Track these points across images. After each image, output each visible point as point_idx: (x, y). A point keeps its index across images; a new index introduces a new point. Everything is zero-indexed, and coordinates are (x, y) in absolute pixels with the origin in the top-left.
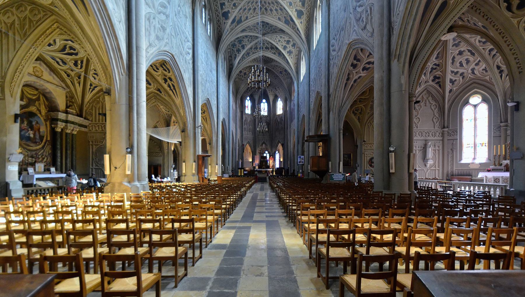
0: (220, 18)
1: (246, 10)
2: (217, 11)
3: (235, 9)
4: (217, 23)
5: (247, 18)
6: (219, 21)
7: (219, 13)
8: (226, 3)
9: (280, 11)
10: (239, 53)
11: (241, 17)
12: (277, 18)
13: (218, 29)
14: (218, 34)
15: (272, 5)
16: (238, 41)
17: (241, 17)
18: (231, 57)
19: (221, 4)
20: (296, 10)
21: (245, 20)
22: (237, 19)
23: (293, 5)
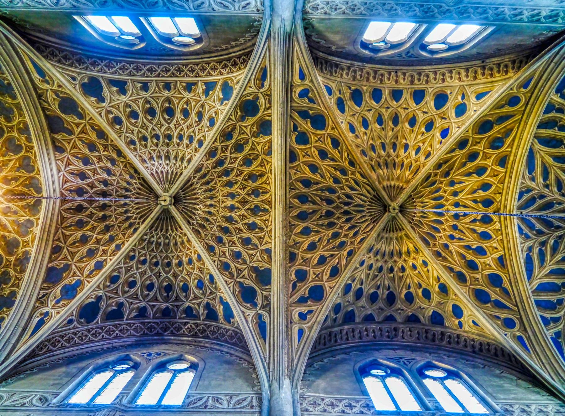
0: (86, 69)
1: (87, 151)
2: (108, 66)
3: (107, 118)
6: (79, 61)
7: (101, 71)
9: (84, 250)
11: (71, 132)
12: (57, 243)
13: (61, 50)
14: (47, 47)
15: (102, 226)
17: (71, 132)
19: (125, 83)
20: (99, 298)
21: (53, 141)
23: (113, 286)
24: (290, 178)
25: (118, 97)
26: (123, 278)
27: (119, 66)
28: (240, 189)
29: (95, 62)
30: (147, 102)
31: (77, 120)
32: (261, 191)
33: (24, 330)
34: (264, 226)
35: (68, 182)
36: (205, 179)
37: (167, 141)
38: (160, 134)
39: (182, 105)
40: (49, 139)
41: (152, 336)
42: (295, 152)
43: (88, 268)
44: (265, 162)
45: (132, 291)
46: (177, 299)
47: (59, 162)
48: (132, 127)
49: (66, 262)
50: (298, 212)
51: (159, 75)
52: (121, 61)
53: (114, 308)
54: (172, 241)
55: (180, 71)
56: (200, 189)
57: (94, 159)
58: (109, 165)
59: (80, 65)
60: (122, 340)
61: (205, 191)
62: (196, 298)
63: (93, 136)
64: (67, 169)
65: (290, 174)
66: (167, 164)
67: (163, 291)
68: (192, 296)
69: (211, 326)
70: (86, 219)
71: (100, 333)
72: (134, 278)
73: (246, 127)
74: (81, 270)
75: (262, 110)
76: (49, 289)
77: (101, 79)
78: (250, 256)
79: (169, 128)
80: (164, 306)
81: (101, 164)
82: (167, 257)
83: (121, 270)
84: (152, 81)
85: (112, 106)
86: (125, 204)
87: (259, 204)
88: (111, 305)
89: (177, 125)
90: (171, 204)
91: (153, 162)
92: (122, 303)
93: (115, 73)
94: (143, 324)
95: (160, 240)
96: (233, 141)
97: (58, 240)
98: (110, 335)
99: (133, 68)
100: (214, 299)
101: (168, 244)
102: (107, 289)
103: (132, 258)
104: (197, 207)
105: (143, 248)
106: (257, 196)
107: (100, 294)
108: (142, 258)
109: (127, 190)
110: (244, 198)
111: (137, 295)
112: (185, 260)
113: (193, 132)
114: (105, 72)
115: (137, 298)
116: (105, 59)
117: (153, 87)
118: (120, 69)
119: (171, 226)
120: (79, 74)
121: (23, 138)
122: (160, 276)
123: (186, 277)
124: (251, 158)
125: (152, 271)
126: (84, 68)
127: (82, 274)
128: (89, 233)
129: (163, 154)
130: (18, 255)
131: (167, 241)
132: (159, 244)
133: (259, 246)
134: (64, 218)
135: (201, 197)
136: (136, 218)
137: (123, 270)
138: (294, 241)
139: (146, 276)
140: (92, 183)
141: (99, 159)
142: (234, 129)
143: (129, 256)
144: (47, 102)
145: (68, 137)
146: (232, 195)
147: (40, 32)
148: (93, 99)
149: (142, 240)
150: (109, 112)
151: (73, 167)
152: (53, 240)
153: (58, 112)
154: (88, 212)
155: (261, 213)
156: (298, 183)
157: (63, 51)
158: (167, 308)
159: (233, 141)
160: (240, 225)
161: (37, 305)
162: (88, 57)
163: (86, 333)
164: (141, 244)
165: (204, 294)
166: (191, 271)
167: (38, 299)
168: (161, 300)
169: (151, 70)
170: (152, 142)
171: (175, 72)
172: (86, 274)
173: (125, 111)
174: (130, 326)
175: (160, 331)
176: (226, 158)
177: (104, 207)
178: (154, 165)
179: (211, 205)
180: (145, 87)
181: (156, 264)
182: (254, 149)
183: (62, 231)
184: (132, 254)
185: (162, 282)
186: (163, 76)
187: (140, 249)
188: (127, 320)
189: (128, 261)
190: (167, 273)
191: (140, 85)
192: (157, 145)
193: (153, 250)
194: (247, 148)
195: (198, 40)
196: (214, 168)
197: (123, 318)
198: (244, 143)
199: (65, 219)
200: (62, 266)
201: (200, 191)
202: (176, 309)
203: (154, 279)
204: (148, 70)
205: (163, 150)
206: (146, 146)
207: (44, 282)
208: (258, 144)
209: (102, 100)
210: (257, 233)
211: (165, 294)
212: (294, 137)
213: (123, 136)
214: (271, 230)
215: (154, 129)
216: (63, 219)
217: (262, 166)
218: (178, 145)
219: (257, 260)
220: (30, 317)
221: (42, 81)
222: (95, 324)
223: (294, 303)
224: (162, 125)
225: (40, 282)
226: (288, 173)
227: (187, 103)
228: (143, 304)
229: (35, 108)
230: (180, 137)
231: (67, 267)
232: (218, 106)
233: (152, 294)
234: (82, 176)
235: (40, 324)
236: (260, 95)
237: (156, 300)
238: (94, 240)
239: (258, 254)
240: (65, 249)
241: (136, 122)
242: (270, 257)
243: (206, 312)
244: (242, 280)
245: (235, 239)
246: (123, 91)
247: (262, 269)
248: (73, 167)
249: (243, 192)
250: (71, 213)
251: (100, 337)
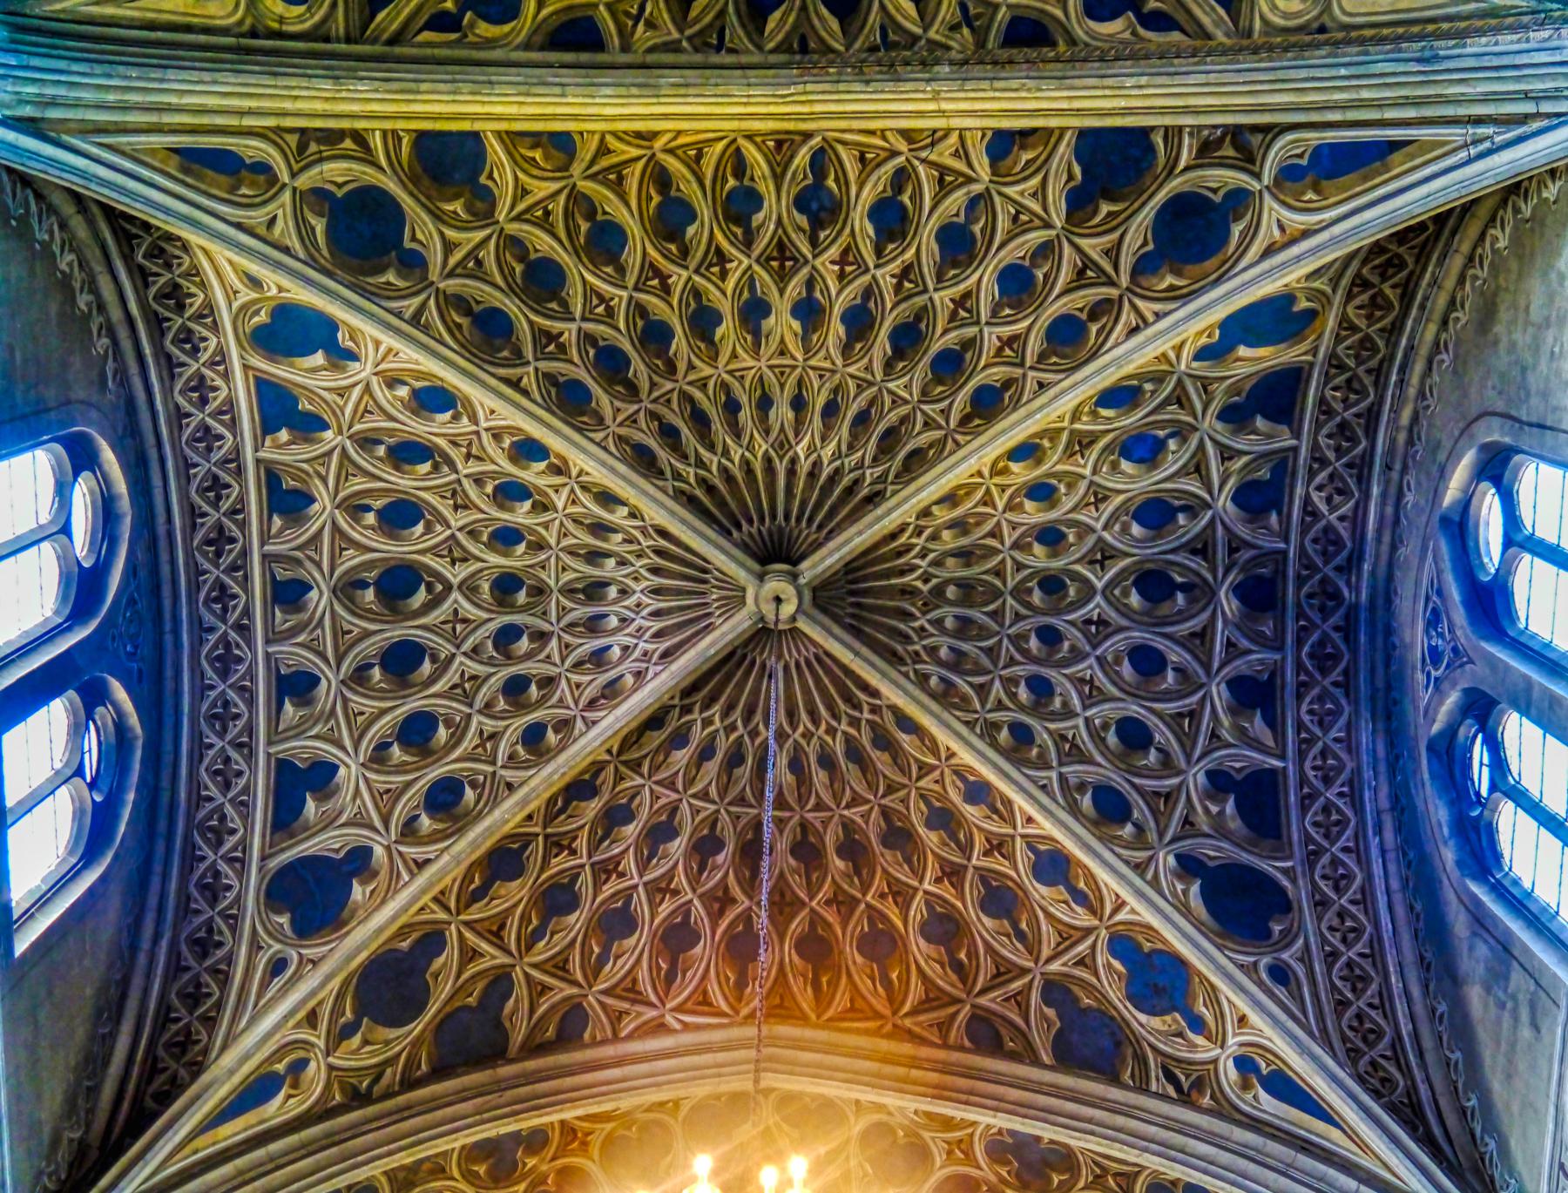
0: (234, 921)
1: (576, 920)
3: (434, 838)
4: (176, 968)
6: (204, 945)
7: (240, 863)
8: (349, 773)
9: (985, 926)
11: (500, 983)
13: (165, 1016)
14: (152, 1068)
15: (888, 860)
17: (500, 983)
19: (283, 768)
20: (1189, 866)
23: (1140, 810)
24: (672, 47)
25: (346, 795)
26: (1105, 771)
27: (214, 791)
28: (724, 275)
29: (203, 887)
30: (359, 676)
31: (449, 957)
32: (732, 182)
33: (1305, 1146)
34: (889, 167)
35: (705, 993)
36: (685, 431)
37: (522, 597)
38: (493, 626)
39: (365, 532)
40: (531, 1064)
41: (1354, 651)
42: (555, 22)
43: (1059, 912)
44: (605, 162)
45: (1162, 734)
46: (1201, 548)
47: (628, 1026)
48: (469, 741)
49: (1035, 997)
50: (824, 11)
51: (244, 629)
52: (195, 784)
53: (1230, 807)
54: (953, 569)
55: (220, 539)
56: (726, 453)
57: (608, 889)
58: (631, 830)
59: (220, 944)
60: (1367, 774)
61: (737, 433)
62: (1198, 468)
63: (514, 894)
64: (653, 998)
65: (651, 50)
66: (624, 592)
67: (1165, 609)
68: (1192, 486)
69: (1322, 401)
70: (860, 922)
71: (1335, 862)
72: (1105, 726)
73: (449, 246)
74: (1069, 936)
75: (370, 176)
76: (1141, 1060)
77: (274, 863)
78: (1019, 226)
79: (469, 588)
80: (1229, 604)
81: (630, 863)
82: (1020, 592)
83: (1073, 780)
84: (268, 656)
85: (386, 822)
86: (796, 765)
87: (790, 191)
88: (1218, 821)
89: (453, 552)
90: (794, 577)
91: (616, 652)
92: (1210, 774)
93: (244, 808)
94: (1302, 689)
95: (949, 623)
96: (512, 307)
97: (943, 1027)
98: (1342, 823)
99: (221, 734)
100: (1205, 384)
101: (965, 586)
102: (1152, 836)
103: (1022, 734)
104: (804, 467)
105: (982, 690)
106: (755, 200)
107: (1171, 860)
108: (1023, 694)
109: (735, 758)
110: (764, 261)
111: (1181, 715)
112: (1033, 514)
113: (478, 481)
114: (244, 845)
115: (1194, 715)
117: (294, 655)
118: (227, 786)
119: (887, 574)
120: (256, 946)
121: (531, 1162)
122: (1102, 622)
123: (1109, 508)
124: (584, 226)
125: (1077, 656)
126: (233, 929)
127: (1088, 931)
128: (917, 908)
129: (581, 612)
130: (1003, 1181)
131: (951, 592)
132: (965, 627)
133: (977, 188)
134: (852, 1009)
135: (762, 446)
136: (855, 723)
137: (1073, 771)
138: (954, 28)
139: (1101, 678)
140: (706, 898)
141: (606, 870)
142: (460, 303)
143: (1015, 750)
144: (378, 1071)
145: (521, 990)
146: (754, 312)
147: (94, 1091)
148: (358, 892)
149: (945, 694)
150: (409, 830)
151: (643, 974)
152: (945, 1046)
153: (417, 1027)
154: (830, 916)
155: (831, 183)
156: (693, 14)
157: (165, 1010)
158: (1239, 590)
159: (512, 307)
160: (885, 277)
161: (1206, 1101)
162: (185, 910)
163: (1330, 917)
164: (965, 699)
165: (1182, 432)
166: (1082, 487)
167: (1185, 1098)
168: (1205, 616)
169: (225, 662)
170: (529, 656)
171: (225, 561)
172: (1083, 918)
173: (401, 768)
174: (1310, 742)
175: (1336, 619)
176: (588, 339)
177: (807, 851)
178: (625, 649)
179: (798, 404)
180: (297, 686)
181: (1050, 637)
182: (547, 213)
183: (907, 1015)
184: (1004, 736)
185: (1125, 611)
186: (247, 612)
187: (983, 703)
188: (1282, 757)
189: (1035, 751)
190: (1088, 591)
191: (288, 707)
192: (541, 637)
193: (989, 651)
194: (543, 243)
195: (81, 457)
196: (632, 391)
197: (1273, 772)
198: (522, 258)
199: (859, 1004)
200: (1050, 1012)
201: (737, 453)
202: (1245, 555)
203: (1113, 645)
204: (224, 674)
205: (563, 611)
206: (548, 682)
207: (1114, 1080)
208: (525, 192)
209: (359, 860)
210: (917, 196)
211: (1180, 598)
212: (485, 29)
213: (509, 775)
214: (906, 134)
215: (475, 650)
216: (856, 1010)
217: (621, 178)
218: (539, 546)
219: (1040, 193)
220: (1254, 1124)
221: (295, 1085)
222: (1294, 881)
223: (1235, 22)
224: (456, 617)
225: (1115, 1093)
226: (651, 58)
227: (355, 509)
228: (1219, 694)
230: (506, 538)
231: (1056, 991)
232: (361, 371)
233: (1175, 655)
234: (678, 937)
235: (1284, 1087)
236: (305, 181)
237: (1203, 636)
238: (946, 891)
239: (1009, 191)
240: (983, 1001)
241: (448, 723)
242: (1024, 136)
243: (1260, 422)
244: (1126, 262)
245: (943, 298)
246: (321, 776)
247: (1077, 170)
248: (643, 974)
249: (740, 263)
250: (834, 984)
251: (1349, 860)
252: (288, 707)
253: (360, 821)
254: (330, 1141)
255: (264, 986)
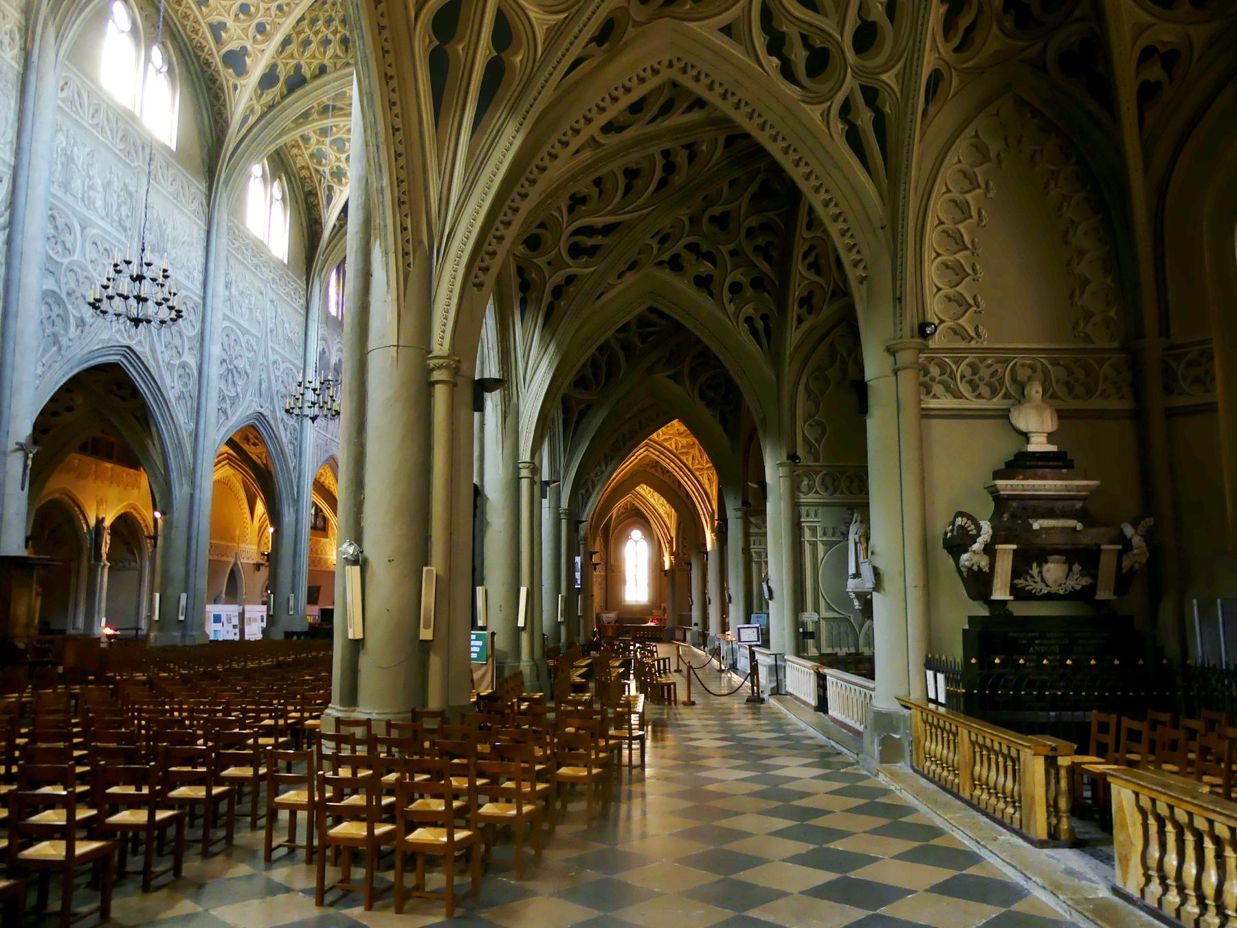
0: (218, 72)
1: (314, 45)
2: (202, 48)
3: (264, 42)
4: (209, 89)
5: (323, 70)
6: (213, 80)
8: (230, 23)
10: (340, 182)
11: (298, 67)
13: (213, 105)
14: (216, 122)
16: (333, 142)
17: (298, 67)
18: (316, 195)
19: (211, 26)
21: (315, 77)
22: (282, 74)
29: (206, 64)
31: (281, 68)
47: (338, 66)
48: (262, 11)
52: (189, 37)
114: (210, 49)
116: (196, 55)
118: (197, 34)
144: (274, 99)
147: (203, 124)
148: (248, 60)
153: (280, 85)
162: (203, 72)
173: (244, 21)
191: (203, 8)
209: (244, 48)
213: (277, 20)
229: (285, 109)
246: (223, 26)
252: (203, 8)
253: (239, 38)
254: (269, 123)
255: (234, 94)
